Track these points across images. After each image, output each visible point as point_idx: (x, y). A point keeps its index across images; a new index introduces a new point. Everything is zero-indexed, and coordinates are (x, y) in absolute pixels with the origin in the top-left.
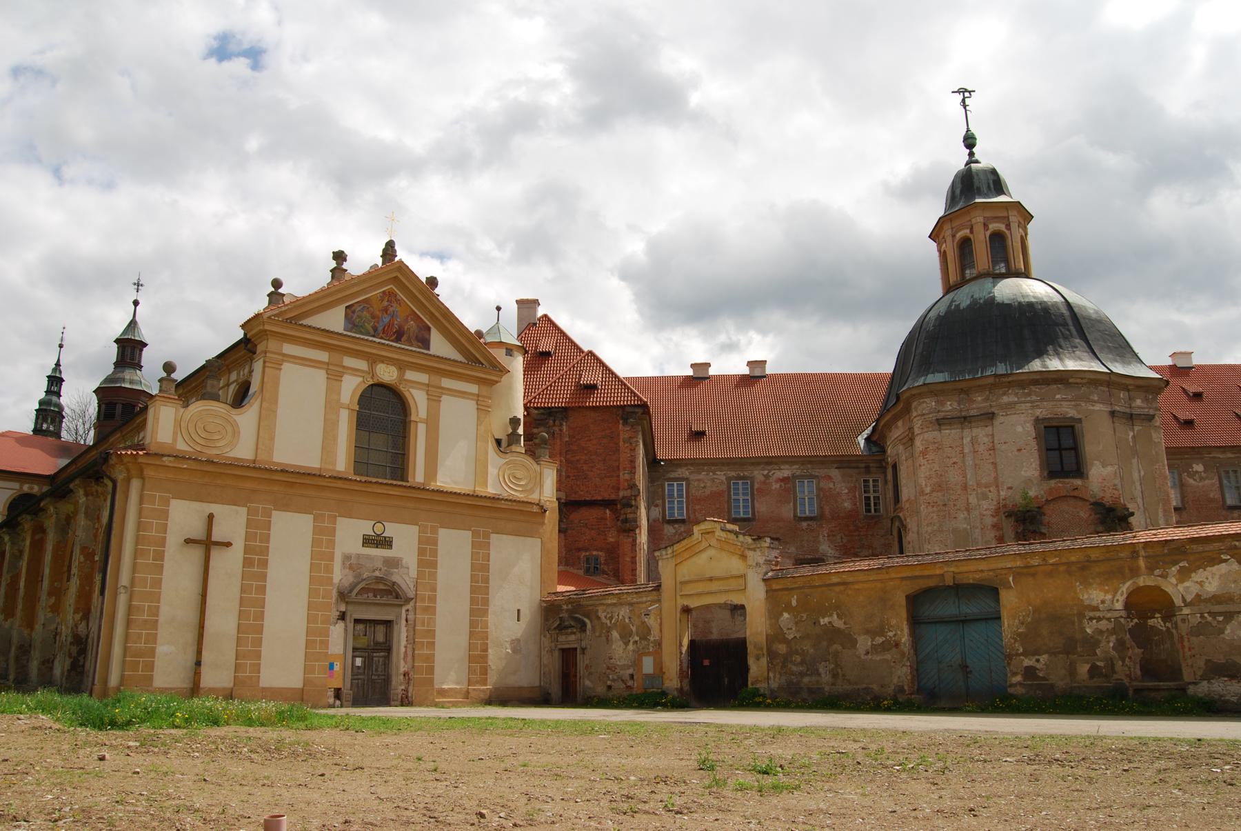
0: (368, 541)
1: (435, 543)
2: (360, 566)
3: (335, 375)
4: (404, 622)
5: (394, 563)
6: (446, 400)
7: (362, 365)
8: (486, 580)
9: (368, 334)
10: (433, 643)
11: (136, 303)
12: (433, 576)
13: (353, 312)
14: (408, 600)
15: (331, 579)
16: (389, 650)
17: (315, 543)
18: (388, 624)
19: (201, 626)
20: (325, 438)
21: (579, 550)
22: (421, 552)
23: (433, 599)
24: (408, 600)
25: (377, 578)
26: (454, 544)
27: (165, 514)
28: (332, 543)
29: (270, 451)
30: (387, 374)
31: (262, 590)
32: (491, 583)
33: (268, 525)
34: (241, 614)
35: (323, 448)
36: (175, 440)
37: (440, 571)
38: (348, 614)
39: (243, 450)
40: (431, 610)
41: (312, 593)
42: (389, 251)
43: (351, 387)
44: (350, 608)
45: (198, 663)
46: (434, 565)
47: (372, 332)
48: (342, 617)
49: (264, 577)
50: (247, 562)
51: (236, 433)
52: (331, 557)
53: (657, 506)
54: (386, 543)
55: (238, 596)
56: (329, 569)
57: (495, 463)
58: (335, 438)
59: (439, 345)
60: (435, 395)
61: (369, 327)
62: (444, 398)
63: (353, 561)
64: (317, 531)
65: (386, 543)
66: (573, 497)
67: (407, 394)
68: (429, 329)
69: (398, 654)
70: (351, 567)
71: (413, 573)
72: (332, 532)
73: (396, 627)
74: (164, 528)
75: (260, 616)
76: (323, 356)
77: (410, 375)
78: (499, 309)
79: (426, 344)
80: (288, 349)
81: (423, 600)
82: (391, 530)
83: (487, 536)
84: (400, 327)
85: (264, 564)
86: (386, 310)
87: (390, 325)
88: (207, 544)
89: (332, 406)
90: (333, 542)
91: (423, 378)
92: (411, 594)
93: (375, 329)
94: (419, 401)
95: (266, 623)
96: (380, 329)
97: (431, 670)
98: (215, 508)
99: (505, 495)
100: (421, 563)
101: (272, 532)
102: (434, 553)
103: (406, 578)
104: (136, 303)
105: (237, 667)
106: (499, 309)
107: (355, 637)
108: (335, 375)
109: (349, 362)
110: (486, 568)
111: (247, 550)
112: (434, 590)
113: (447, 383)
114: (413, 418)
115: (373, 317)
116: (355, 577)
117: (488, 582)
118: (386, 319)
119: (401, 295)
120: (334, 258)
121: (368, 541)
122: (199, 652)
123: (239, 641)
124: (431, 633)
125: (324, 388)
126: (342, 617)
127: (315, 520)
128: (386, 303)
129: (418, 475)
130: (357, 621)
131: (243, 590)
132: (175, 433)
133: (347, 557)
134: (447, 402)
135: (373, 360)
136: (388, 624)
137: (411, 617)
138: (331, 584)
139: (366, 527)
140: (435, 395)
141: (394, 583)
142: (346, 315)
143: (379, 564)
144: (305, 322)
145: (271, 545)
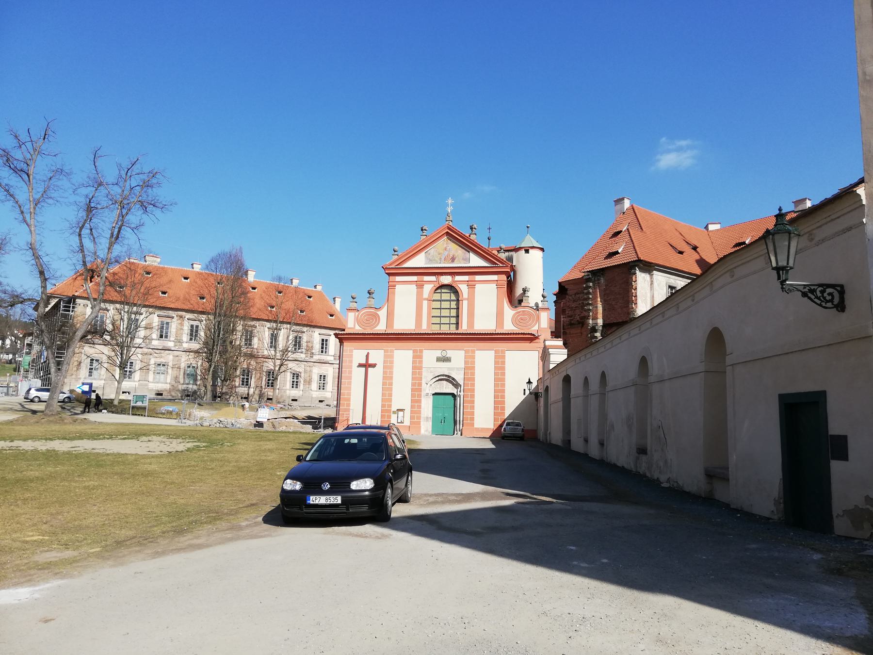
0: (439, 360)
3: (420, 286)
6: (478, 287)
7: (433, 278)
9: (437, 263)
27: (351, 356)
30: (446, 280)
43: (428, 289)
57: (509, 312)
65: (447, 360)
66: (608, 322)
72: (421, 357)
74: (351, 362)
76: (415, 278)
77: (458, 278)
82: (449, 353)
88: (367, 366)
91: (466, 278)
94: (463, 289)
97: (472, 419)
108: (420, 286)
109: (426, 278)
113: (478, 278)
118: (446, 253)
121: (439, 360)
139: (438, 353)
140: (471, 286)
142: (426, 257)
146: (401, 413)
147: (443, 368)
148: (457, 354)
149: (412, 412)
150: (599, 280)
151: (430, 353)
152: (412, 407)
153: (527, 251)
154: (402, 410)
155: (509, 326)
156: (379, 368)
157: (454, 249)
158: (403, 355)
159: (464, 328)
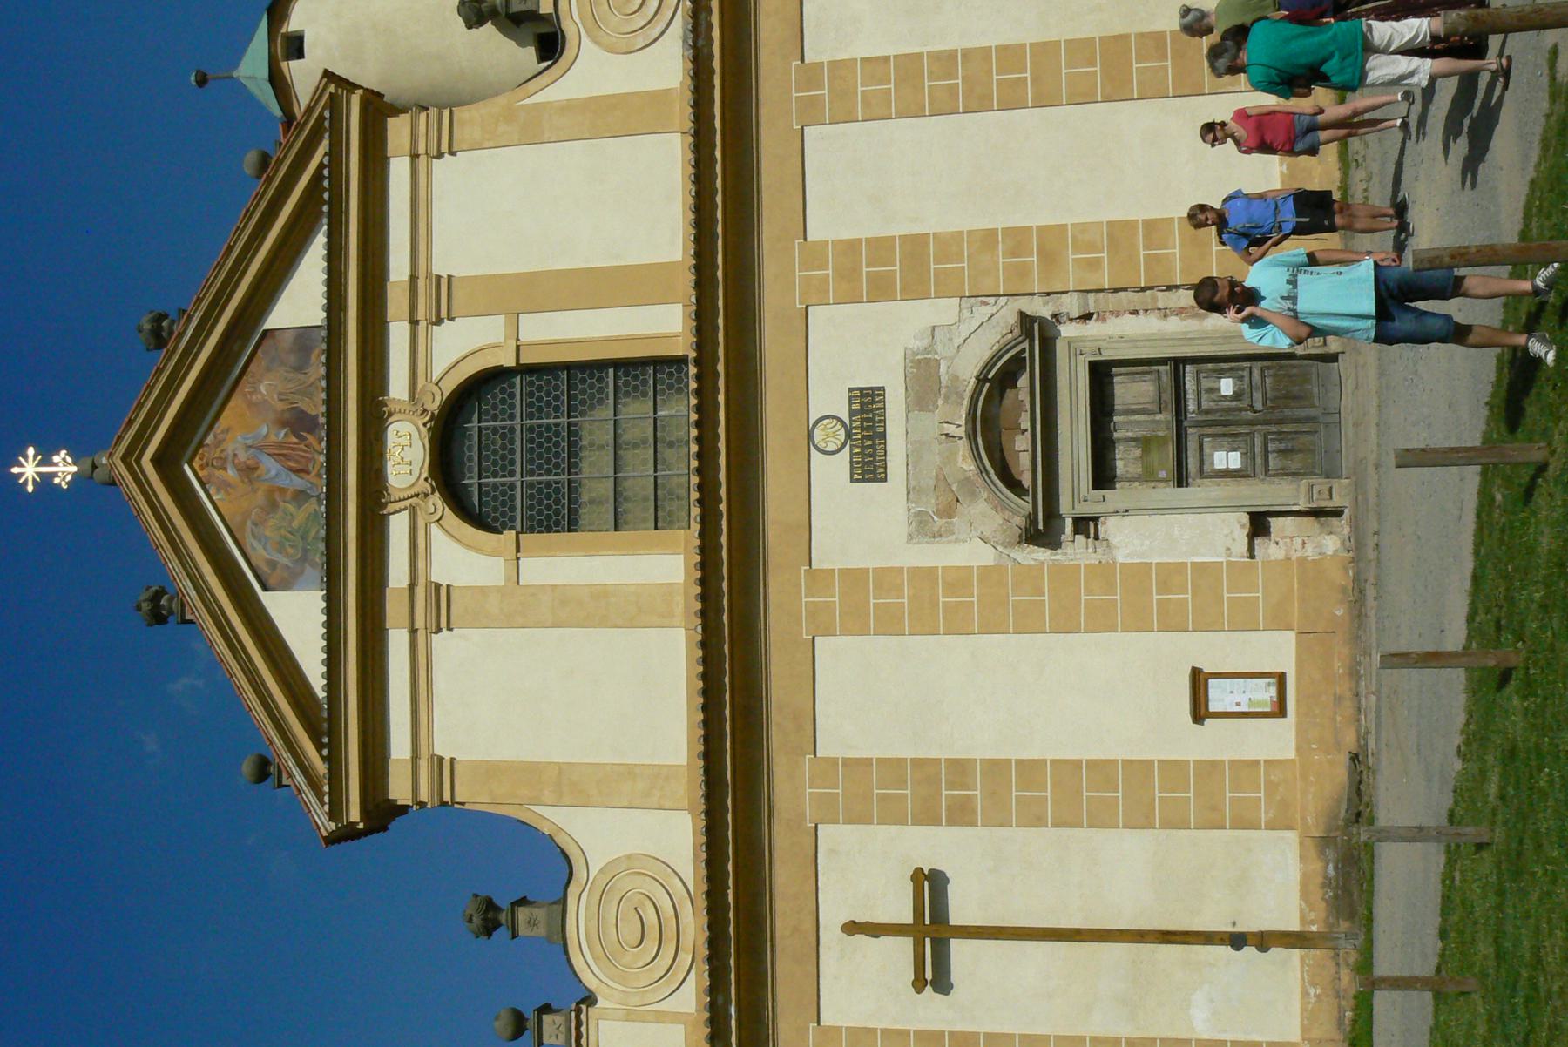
0: (869, 467)
1: (852, 246)
2: (941, 480)
3: (440, 607)
4: (1092, 329)
5: (924, 377)
7: (398, 527)
8: (946, 60)
10: (1149, 224)
12: (949, 244)
13: (273, 564)
14: (1026, 321)
15: (985, 571)
16: (1178, 363)
17: (890, 624)
18: (1101, 374)
19: (1139, 936)
20: (604, 622)
22: (881, 291)
23: (1017, 238)
24: (1026, 321)
25: (971, 437)
26: (842, 182)
28: (886, 578)
29: (660, 775)
30: (407, 453)
31: (1030, 770)
32: (953, 42)
33: (858, 766)
34: (1101, 819)
35: (631, 624)
36: (676, 1017)
37: (935, 219)
38: (1084, 510)
39: (675, 838)
40: (1050, 243)
41: (1027, 622)
43: (458, 557)
44: (1067, 507)
45: (1237, 941)
46: (916, 245)
48: (1084, 525)
49: (996, 768)
50: (961, 815)
51: (632, 864)
52: (925, 576)
54: (868, 403)
55: (1050, 833)
56: (958, 580)
57: (589, 71)
58: (601, 593)
60: (441, 300)
62: (439, 268)
63: (929, 505)
64: (857, 623)
65: (868, 403)
67: (449, 386)
68: (266, 331)
69: (1187, 339)
70: (948, 512)
71: (942, 310)
72: (854, 578)
73: (1107, 355)
75: (1102, 769)
76: (397, 642)
77: (398, 387)
80: (399, 746)
81: (1023, 272)
82: (829, 399)
83: (811, 76)
84: (283, 424)
85: (960, 768)
86: (249, 471)
89: (518, 608)
90: (881, 573)
92: (1007, 314)
93: (300, 496)
94: (462, 345)
95: (1120, 754)
96: (297, 482)
98: (833, 916)
99: (678, 27)
100: (916, 289)
101: (875, 753)
102: (880, 247)
103: (965, 329)
105: (1244, 822)
107: (1148, 477)
108: (440, 607)
110: (909, 65)
111: (927, 816)
112: (989, 237)
114: (509, 361)
115: (272, 506)
116: (973, 495)
117: (951, 55)
118: (270, 466)
121: (869, 467)
122: (1207, 938)
123: (1176, 822)
124: (1119, 232)
125: (476, 635)
126: (1084, 525)
127: (829, 632)
128: (231, 474)
129: (666, 325)
130: (1103, 477)
131: (1038, 822)
132: (661, 1017)
133: (921, 528)
136: (1101, 374)
137: (1071, 304)
138: (998, 569)
139: (831, 470)
140: (441, 300)
141: (981, 380)
142: (285, 585)
143: (929, 423)
145: (908, 753)
146: (1221, 696)
147: (926, 439)
148: (836, 350)
149: (1206, 624)
151: (840, 522)
152: (1172, 622)
154: (1199, 681)
155: (664, 67)
156: (934, 846)
157: (244, 427)
158: (853, 696)
159: (666, 325)
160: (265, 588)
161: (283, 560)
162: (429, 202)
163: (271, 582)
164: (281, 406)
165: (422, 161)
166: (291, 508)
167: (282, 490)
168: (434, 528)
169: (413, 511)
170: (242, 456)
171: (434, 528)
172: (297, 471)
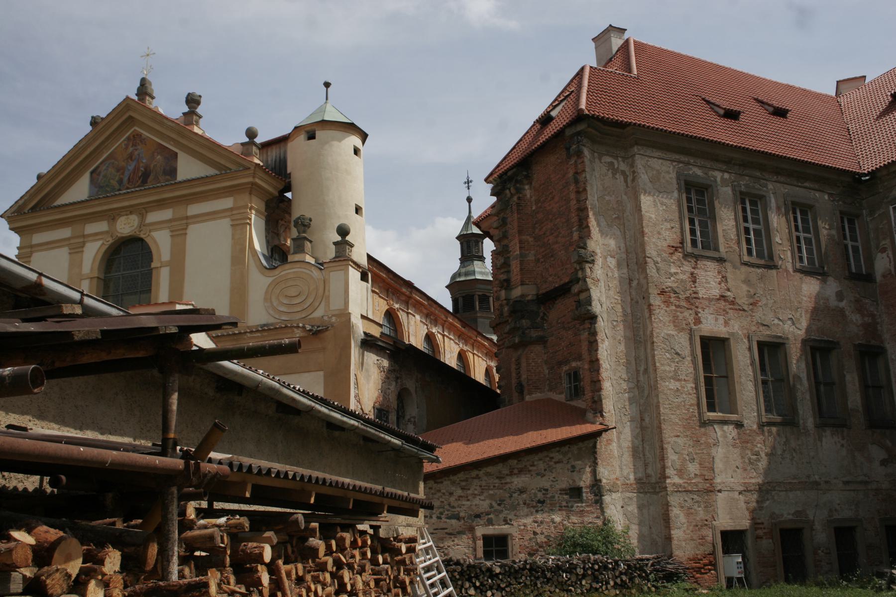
7: (102, 226)
11: (469, 200)
13: (99, 175)
21: (560, 364)
30: (126, 226)
42: (144, 90)
43: (93, 252)
47: (117, 187)
53: (884, 250)
57: (259, 283)
59: (188, 168)
61: (114, 183)
67: (148, 240)
68: (176, 154)
77: (153, 217)
78: (327, 85)
79: (173, 172)
86: (131, 157)
87: (136, 169)
91: (166, 214)
94: (161, 242)
96: (125, 179)
104: (469, 200)
106: (327, 85)
108: (76, 247)
113: (194, 209)
115: (118, 171)
118: (131, 168)
119: (146, 134)
120: (91, 124)
128: (131, 149)
134: (195, 232)
135: (111, 216)
142: (92, 181)
144: (59, 202)
150: (518, 191)
153: (311, 136)
160: (92, 173)
161: (101, 177)
162: (214, 219)
163: (94, 175)
164: (152, 166)
165: (229, 213)
166: (117, 178)
167: (123, 174)
168: (100, 242)
169: (107, 232)
170: (136, 153)
171: (100, 242)
172: (129, 179)
